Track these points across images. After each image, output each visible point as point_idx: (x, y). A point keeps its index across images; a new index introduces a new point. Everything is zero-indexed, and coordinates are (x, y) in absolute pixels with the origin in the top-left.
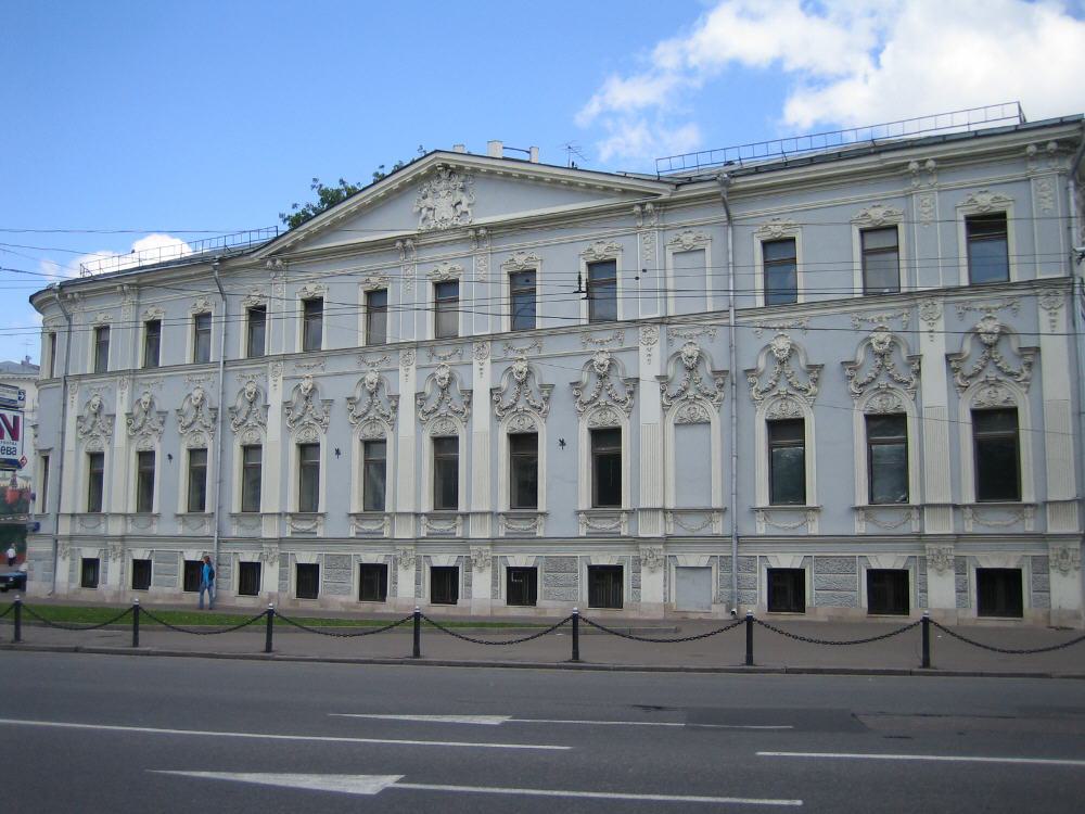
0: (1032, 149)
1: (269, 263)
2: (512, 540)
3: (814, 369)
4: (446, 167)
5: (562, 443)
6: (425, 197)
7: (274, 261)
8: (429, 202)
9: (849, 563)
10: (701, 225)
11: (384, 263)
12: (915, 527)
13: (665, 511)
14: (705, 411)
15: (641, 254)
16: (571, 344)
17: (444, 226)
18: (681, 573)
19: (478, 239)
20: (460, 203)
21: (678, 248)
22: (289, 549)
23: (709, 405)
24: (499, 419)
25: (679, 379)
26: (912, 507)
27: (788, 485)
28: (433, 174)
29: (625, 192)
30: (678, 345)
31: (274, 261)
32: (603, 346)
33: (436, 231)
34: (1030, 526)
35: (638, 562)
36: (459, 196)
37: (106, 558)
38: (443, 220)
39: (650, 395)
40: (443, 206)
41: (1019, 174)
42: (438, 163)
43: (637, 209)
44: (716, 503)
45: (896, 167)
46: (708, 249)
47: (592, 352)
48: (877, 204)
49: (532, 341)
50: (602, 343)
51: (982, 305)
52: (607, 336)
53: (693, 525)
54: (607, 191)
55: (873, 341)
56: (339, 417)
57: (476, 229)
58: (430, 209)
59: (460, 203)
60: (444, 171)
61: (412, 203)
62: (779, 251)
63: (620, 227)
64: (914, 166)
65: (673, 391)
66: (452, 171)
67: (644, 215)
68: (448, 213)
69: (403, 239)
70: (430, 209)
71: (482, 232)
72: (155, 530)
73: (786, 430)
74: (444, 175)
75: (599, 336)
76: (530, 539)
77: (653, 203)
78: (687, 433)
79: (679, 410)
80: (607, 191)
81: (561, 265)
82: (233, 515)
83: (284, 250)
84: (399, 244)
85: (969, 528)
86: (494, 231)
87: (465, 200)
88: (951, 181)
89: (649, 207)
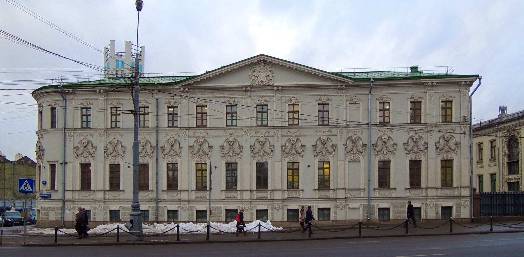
1: (182, 89)
2: (290, 199)
3: (395, 145)
5: (309, 166)
6: (254, 71)
7: (184, 89)
8: (255, 74)
12: (424, 194)
13: (346, 189)
14: (359, 157)
16: (313, 132)
17: (262, 84)
18: (350, 210)
19: (277, 90)
21: (351, 102)
22: (192, 204)
23: (360, 156)
24: (285, 157)
25: (350, 145)
26: (423, 188)
27: (384, 181)
31: (184, 89)
33: (260, 86)
35: (335, 206)
43: (339, 87)
45: (423, 83)
46: (361, 103)
48: (417, 93)
49: (298, 130)
50: (324, 132)
53: (355, 193)
54: (329, 79)
55: (414, 138)
57: (278, 87)
58: (256, 76)
63: (332, 92)
64: (430, 83)
65: (348, 150)
67: (342, 89)
68: (264, 80)
69: (246, 87)
70: (256, 76)
71: (280, 88)
75: (323, 130)
76: (297, 199)
79: (350, 156)
80: (329, 79)
82: (163, 191)
83: (190, 84)
84: (244, 88)
85: (439, 194)
87: (271, 76)
89: (344, 86)
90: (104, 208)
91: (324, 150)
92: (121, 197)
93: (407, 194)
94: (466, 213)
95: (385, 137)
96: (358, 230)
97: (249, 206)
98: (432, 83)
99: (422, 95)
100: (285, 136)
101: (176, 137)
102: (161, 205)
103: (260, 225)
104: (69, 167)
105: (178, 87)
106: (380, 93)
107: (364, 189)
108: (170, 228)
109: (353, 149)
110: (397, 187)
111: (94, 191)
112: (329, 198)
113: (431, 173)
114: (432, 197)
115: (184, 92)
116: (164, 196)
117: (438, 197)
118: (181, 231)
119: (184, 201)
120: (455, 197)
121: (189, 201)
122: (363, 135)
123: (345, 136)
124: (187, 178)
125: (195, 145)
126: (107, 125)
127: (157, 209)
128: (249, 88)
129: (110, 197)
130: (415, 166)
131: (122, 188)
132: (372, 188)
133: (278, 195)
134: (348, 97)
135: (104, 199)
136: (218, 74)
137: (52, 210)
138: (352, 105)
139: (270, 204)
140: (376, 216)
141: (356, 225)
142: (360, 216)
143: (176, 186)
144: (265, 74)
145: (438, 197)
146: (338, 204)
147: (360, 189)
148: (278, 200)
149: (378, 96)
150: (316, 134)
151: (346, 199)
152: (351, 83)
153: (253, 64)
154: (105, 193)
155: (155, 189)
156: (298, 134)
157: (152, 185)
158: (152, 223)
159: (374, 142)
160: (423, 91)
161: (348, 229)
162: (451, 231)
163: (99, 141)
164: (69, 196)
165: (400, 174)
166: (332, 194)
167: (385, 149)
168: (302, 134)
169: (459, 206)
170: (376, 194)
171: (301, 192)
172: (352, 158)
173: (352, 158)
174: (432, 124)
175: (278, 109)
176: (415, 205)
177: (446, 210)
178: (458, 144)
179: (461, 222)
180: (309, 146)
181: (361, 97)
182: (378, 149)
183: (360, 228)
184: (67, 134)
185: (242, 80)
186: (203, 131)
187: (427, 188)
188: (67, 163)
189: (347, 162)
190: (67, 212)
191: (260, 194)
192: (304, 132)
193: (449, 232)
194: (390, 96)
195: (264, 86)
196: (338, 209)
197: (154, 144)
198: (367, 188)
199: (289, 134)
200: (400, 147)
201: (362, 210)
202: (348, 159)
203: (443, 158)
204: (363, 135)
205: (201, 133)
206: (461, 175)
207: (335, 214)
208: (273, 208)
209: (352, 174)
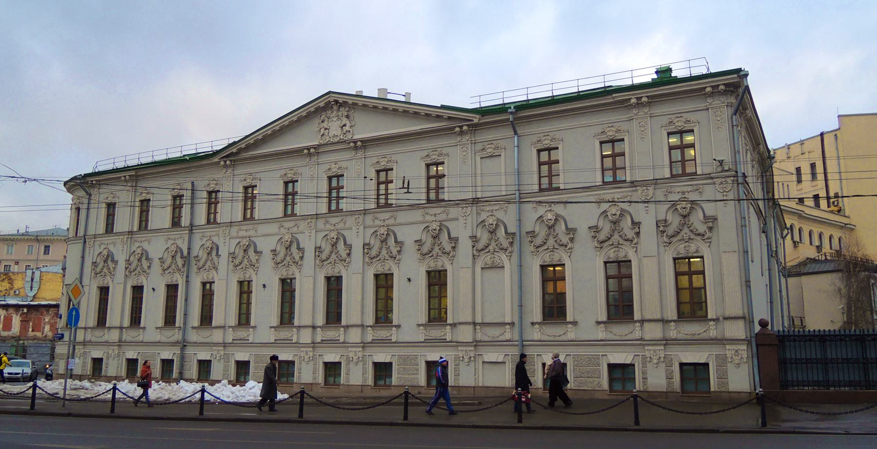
0: (709, 89)
1: (222, 163)
4: (336, 102)
7: (225, 162)
8: (325, 125)
9: (594, 361)
12: (637, 334)
14: (500, 259)
17: (336, 140)
18: (486, 365)
19: (356, 148)
20: (345, 125)
21: (484, 154)
22: (230, 350)
23: (504, 257)
25: (484, 237)
27: (555, 309)
28: (328, 107)
29: (450, 118)
30: (484, 216)
31: (225, 162)
32: (246, 231)
35: (457, 358)
36: (345, 121)
37: (108, 358)
38: (334, 136)
41: (702, 105)
42: (332, 99)
43: (457, 129)
44: (508, 320)
46: (503, 154)
47: (428, 222)
50: (435, 215)
51: (679, 189)
55: (609, 214)
56: (267, 261)
57: (355, 142)
58: (326, 129)
59: (345, 125)
64: (633, 101)
65: (480, 245)
67: (462, 133)
68: (338, 132)
70: (326, 129)
74: (335, 108)
77: (468, 125)
78: (490, 274)
79: (485, 259)
81: (409, 165)
82: (193, 328)
83: (232, 154)
84: (306, 151)
85: (673, 334)
86: (367, 144)
87: (348, 124)
88: (658, 110)
89: (465, 128)
90: (118, 356)
91: (436, 249)
93: (601, 333)
95: (550, 216)
96: (403, 407)
97: (311, 354)
98: (639, 99)
99: (624, 126)
100: (370, 227)
102: (189, 351)
103: (203, 391)
105: (216, 160)
106: (538, 132)
107: (512, 324)
108: (187, 390)
109: (494, 242)
110: (577, 319)
111: (109, 328)
112: (444, 341)
113: (653, 290)
114: (654, 342)
115: (225, 166)
117: (667, 342)
118: (207, 397)
119: (216, 344)
121: (225, 345)
122: (509, 216)
124: (225, 308)
125: (237, 251)
126: (133, 226)
127: (183, 358)
128: (312, 150)
129: (129, 339)
130: (619, 275)
131: (142, 325)
132: (528, 320)
133: (355, 336)
134: (479, 147)
135: (120, 341)
136: (269, 132)
138: (488, 161)
139: (342, 351)
141: (397, 397)
143: (210, 322)
144: (339, 122)
145: (667, 342)
146: (461, 354)
147: (503, 324)
148: (355, 345)
149: (535, 139)
150: (421, 219)
152: (476, 119)
153: (318, 111)
154: (121, 332)
156: (391, 221)
158: (177, 381)
159: (528, 227)
160: (625, 117)
161: (383, 404)
162: (637, 422)
165: (587, 293)
167: (551, 242)
168: (399, 221)
169: (722, 361)
171: (394, 329)
172: (489, 262)
173: (489, 262)
174: (645, 183)
175: (358, 181)
176: (562, 358)
177: (695, 373)
178: (711, 221)
181: (502, 143)
183: (406, 404)
184: (87, 245)
185: (306, 137)
186: (250, 227)
189: (478, 270)
191: (379, 332)
192: (402, 217)
193: (630, 422)
194: (558, 135)
195: (338, 142)
196: (461, 363)
197: (185, 253)
198: (516, 320)
199: (377, 222)
202: (479, 265)
203: (679, 253)
204: (509, 216)
206: (723, 294)
208: (349, 361)
209: (492, 293)
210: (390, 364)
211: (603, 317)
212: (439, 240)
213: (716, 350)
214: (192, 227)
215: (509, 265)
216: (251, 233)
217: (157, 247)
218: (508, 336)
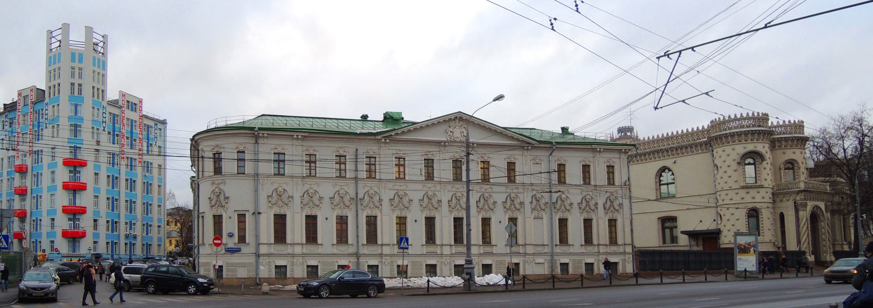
8: (451, 129)
9: (580, 262)
10: (543, 154)
11: (433, 149)
15: (524, 163)
17: (458, 140)
22: (394, 259)
23: (543, 213)
27: (564, 240)
34: (621, 250)
35: (524, 262)
36: (463, 130)
39: (528, 207)
40: (458, 133)
52: (459, 186)
53: (540, 249)
56: (415, 207)
60: (460, 119)
61: (445, 127)
62: (561, 168)
63: (517, 152)
66: (461, 119)
72: (320, 250)
73: (563, 223)
79: (535, 213)
81: (499, 161)
92: (320, 251)
93: (583, 250)
94: (629, 268)
101: (376, 189)
102: (362, 260)
104: (263, 218)
115: (385, 143)
116: (364, 250)
120: (621, 253)
123: (530, 194)
137: (243, 265)
140: (558, 271)
142: (544, 270)
147: (544, 245)
151: (534, 254)
155: (355, 243)
157: (351, 238)
163: (296, 190)
164: (263, 250)
166: (521, 250)
169: (624, 261)
170: (558, 250)
178: (621, 205)
179: (626, 276)
180: (499, 202)
182: (558, 206)
185: (437, 135)
187: (598, 245)
188: (259, 213)
190: (262, 268)
197: (353, 194)
198: (550, 244)
200: (575, 206)
201: (546, 265)
205: (400, 185)
207: (524, 269)
210: (491, 265)
211: (583, 243)
212: (511, 203)
213: (622, 257)
214: (356, 179)
215: (546, 216)
216: (404, 187)
217: (326, 190)
218: (546, 251)
